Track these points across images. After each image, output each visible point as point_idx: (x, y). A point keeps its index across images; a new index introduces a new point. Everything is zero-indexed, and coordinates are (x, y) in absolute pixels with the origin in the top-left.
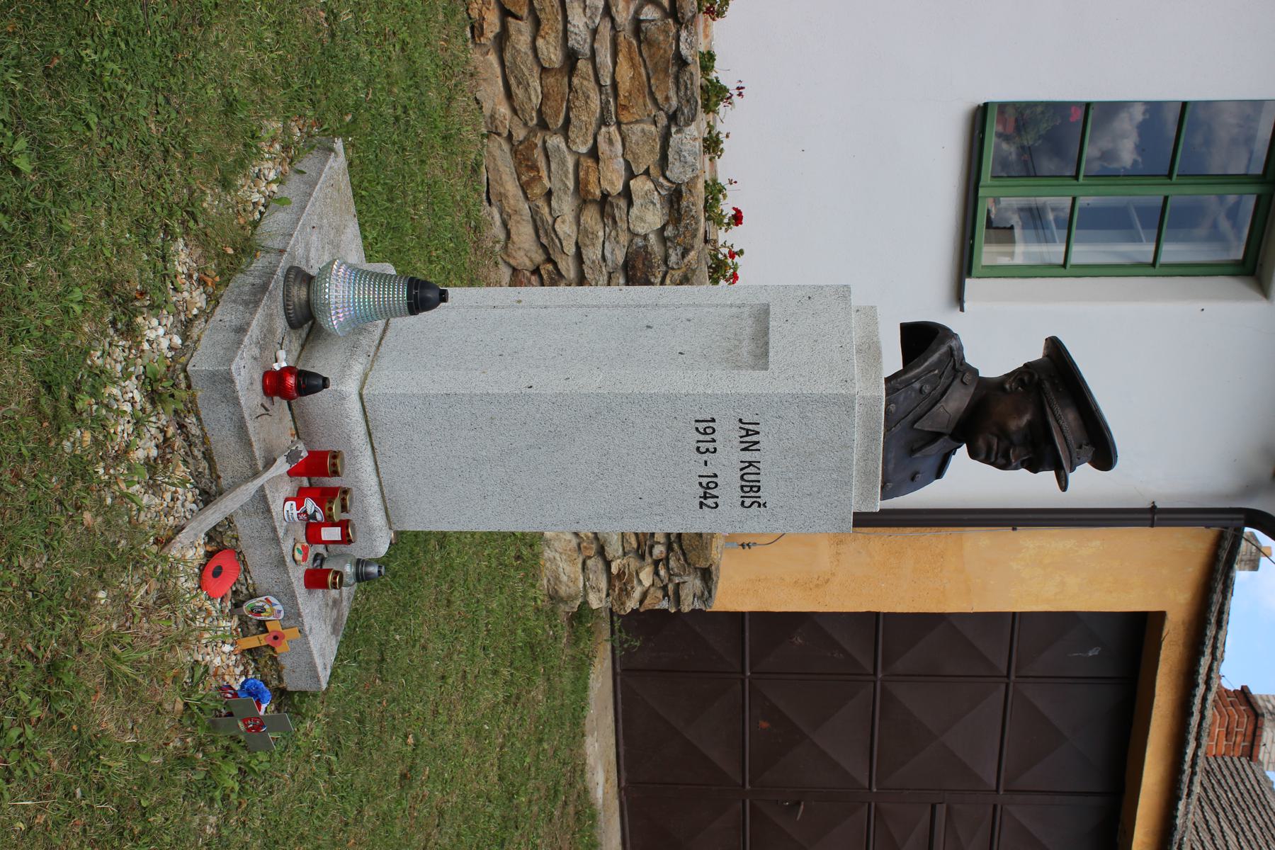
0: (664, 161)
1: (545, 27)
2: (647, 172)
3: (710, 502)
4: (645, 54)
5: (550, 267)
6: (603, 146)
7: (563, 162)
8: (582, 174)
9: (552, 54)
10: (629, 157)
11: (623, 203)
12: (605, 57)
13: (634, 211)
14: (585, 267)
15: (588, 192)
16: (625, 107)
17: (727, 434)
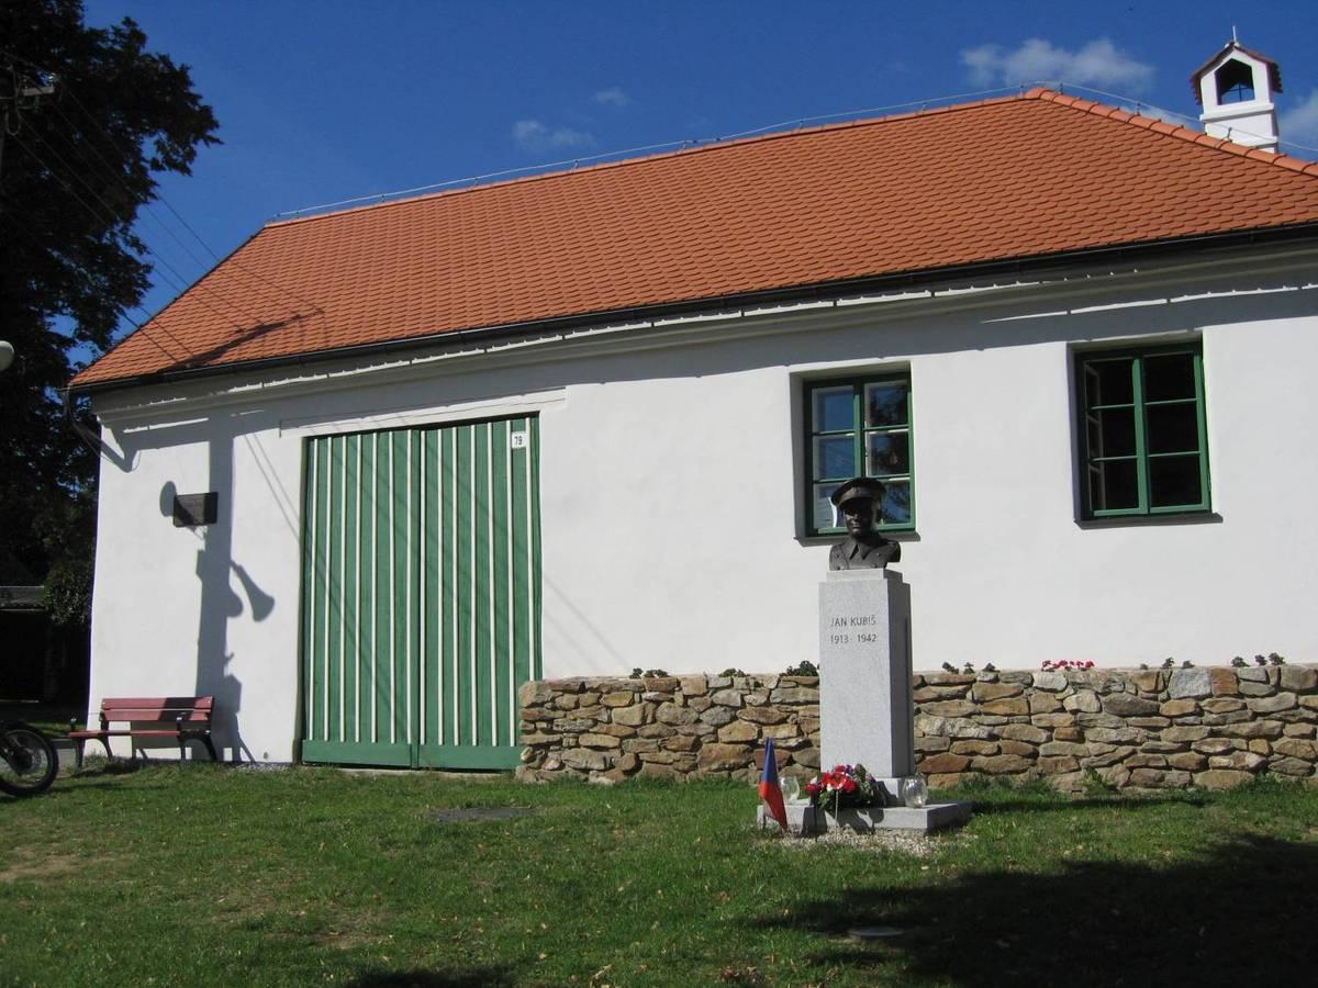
0: (1054, 691)
1: (976, 749)
2: (1062, 700)
3: (872, 638)
4: (991, 698)
5: (1125, 761)
6: (1043, 724)
7: (1054, 747)
8: (1061, 737)
9: (990, 747)
10: (1050, 710)
11: (1079, 714)
12: (991, 719)
13: (1083, 709)
14: (1123, 740)
15: (1072, 734)
16: (1020, 711)
17: (838, 631)
